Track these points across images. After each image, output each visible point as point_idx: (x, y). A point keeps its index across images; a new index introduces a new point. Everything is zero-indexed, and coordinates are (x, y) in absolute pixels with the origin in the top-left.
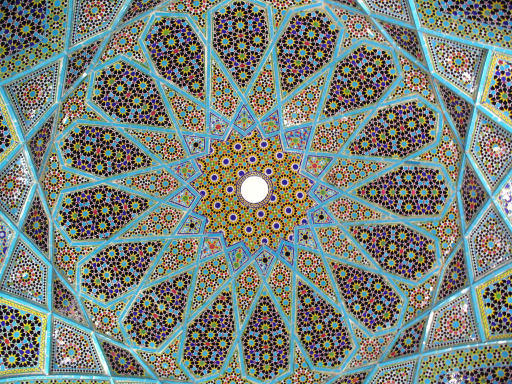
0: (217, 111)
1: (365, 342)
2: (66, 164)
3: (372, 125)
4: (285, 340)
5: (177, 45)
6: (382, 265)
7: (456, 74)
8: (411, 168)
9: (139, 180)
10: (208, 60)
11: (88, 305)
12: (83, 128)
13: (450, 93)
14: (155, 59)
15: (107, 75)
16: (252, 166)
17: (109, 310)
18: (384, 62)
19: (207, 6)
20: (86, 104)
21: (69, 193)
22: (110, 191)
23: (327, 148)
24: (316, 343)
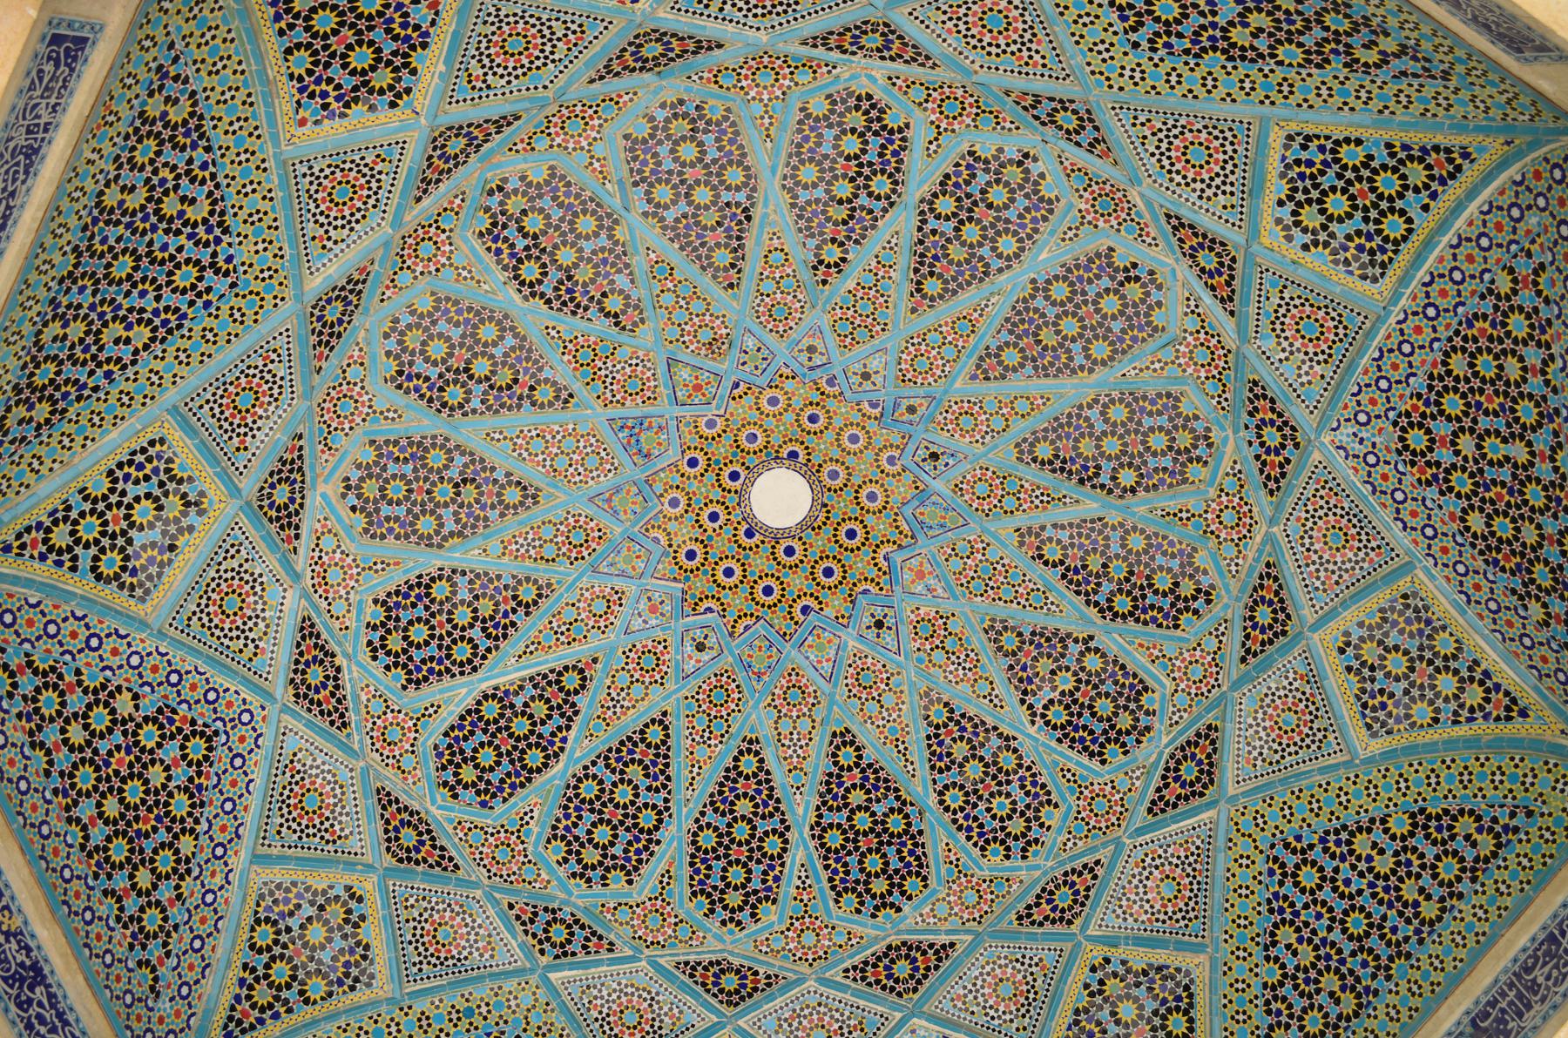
4: (1113, 401)
5: (490, 743)
6: (892, 204)
14: (529, 780)
15: (578, 869)
20: (643, 898)
22: (820, 816)
24: (1109, 330)
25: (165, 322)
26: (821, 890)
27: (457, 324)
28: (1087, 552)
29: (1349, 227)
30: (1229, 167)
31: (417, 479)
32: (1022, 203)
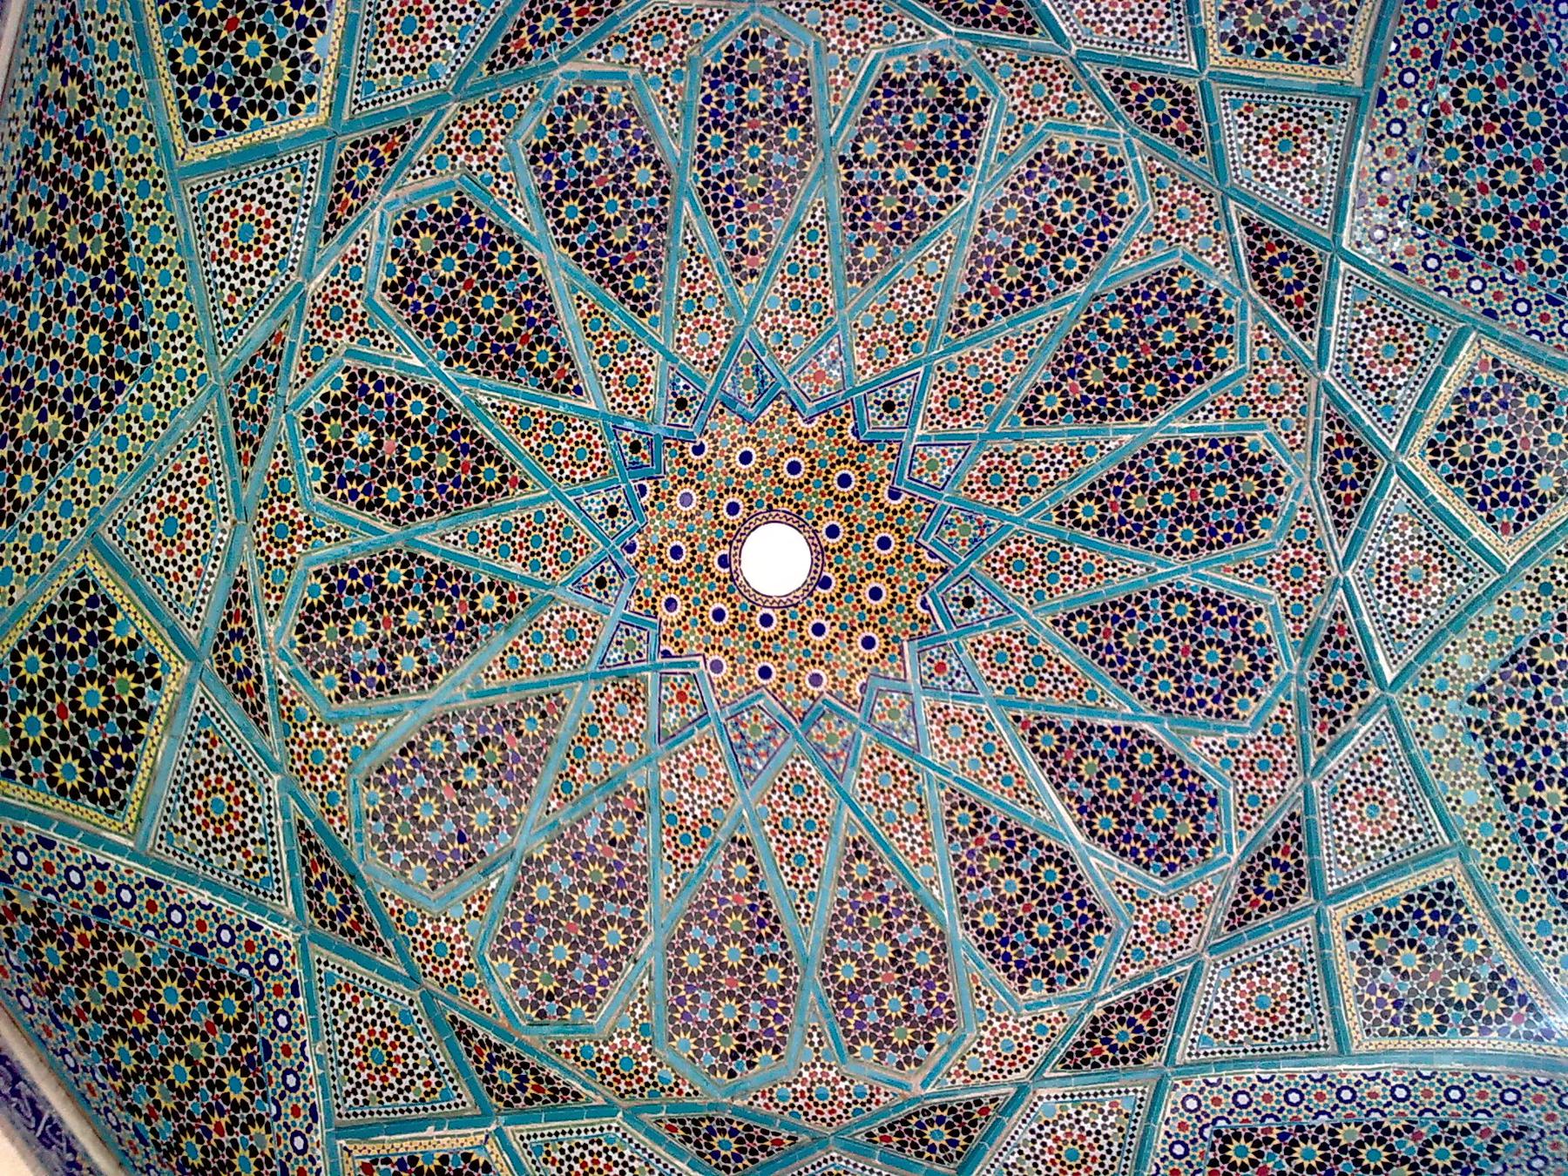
1: (356, 326)
2: (1257, 440)
3: (636, 885)
4: (560, 223)
5: (1144, 814)
6: (412, 556)
7: (577, 1152)
9: (1067, 465)
10: (1058, 813)
11: (1093, 113)
12: (1254, 534)
14: (1172, 758)
16: (809, 613)
17: (1036, 118)
19: (1138, 935)
21: (1227, 373)
22: (1128, 414)
24: (478, 256)
26: (1213, 389)
27: (695, 999)
29: (276, 25)
30: (249, 192)
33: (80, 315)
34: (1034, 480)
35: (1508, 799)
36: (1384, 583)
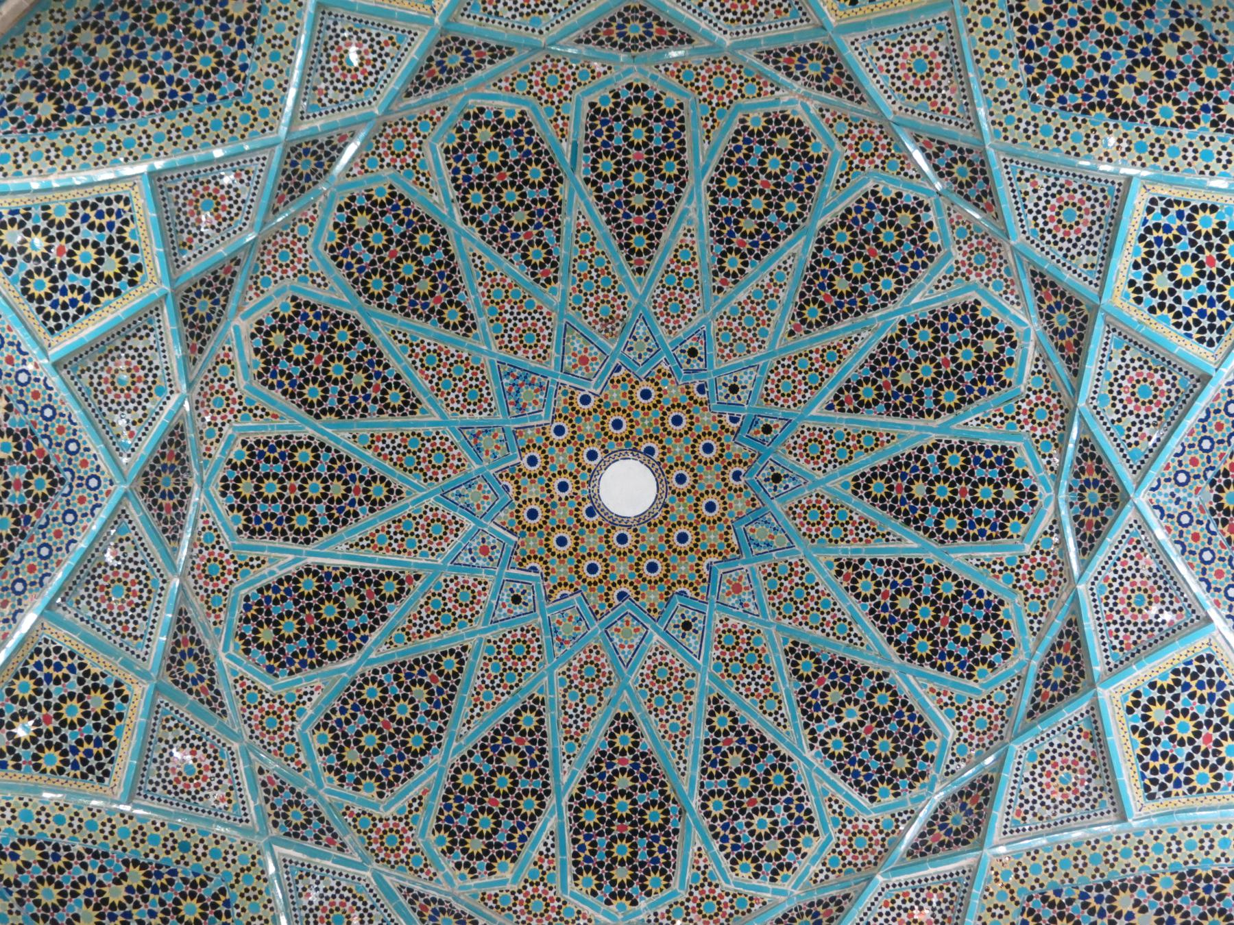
0: (448, 550)
1: (963, 270)
2: (508, 875)
4: (951, 448)
5: (296, 616)
6: (795, 227)
7: (378, 64)
8: (584, 161)
11: (822, 876)
13: (419, 78)
14: (320, 663)
15: (336, 764)
18: (361, 209)
21: (570, 879)
22: (582, 790)
23: (546, 332)
24: (961, 379)
25: (173, 94)
26: (563, 863)
28: (898, 592)
30: (1096, 228)
31: (320, 348)
32: (908, 247)
33: (1092, 59)
34: (574, 697)
35: (136, 863)
36: (346, 894)
